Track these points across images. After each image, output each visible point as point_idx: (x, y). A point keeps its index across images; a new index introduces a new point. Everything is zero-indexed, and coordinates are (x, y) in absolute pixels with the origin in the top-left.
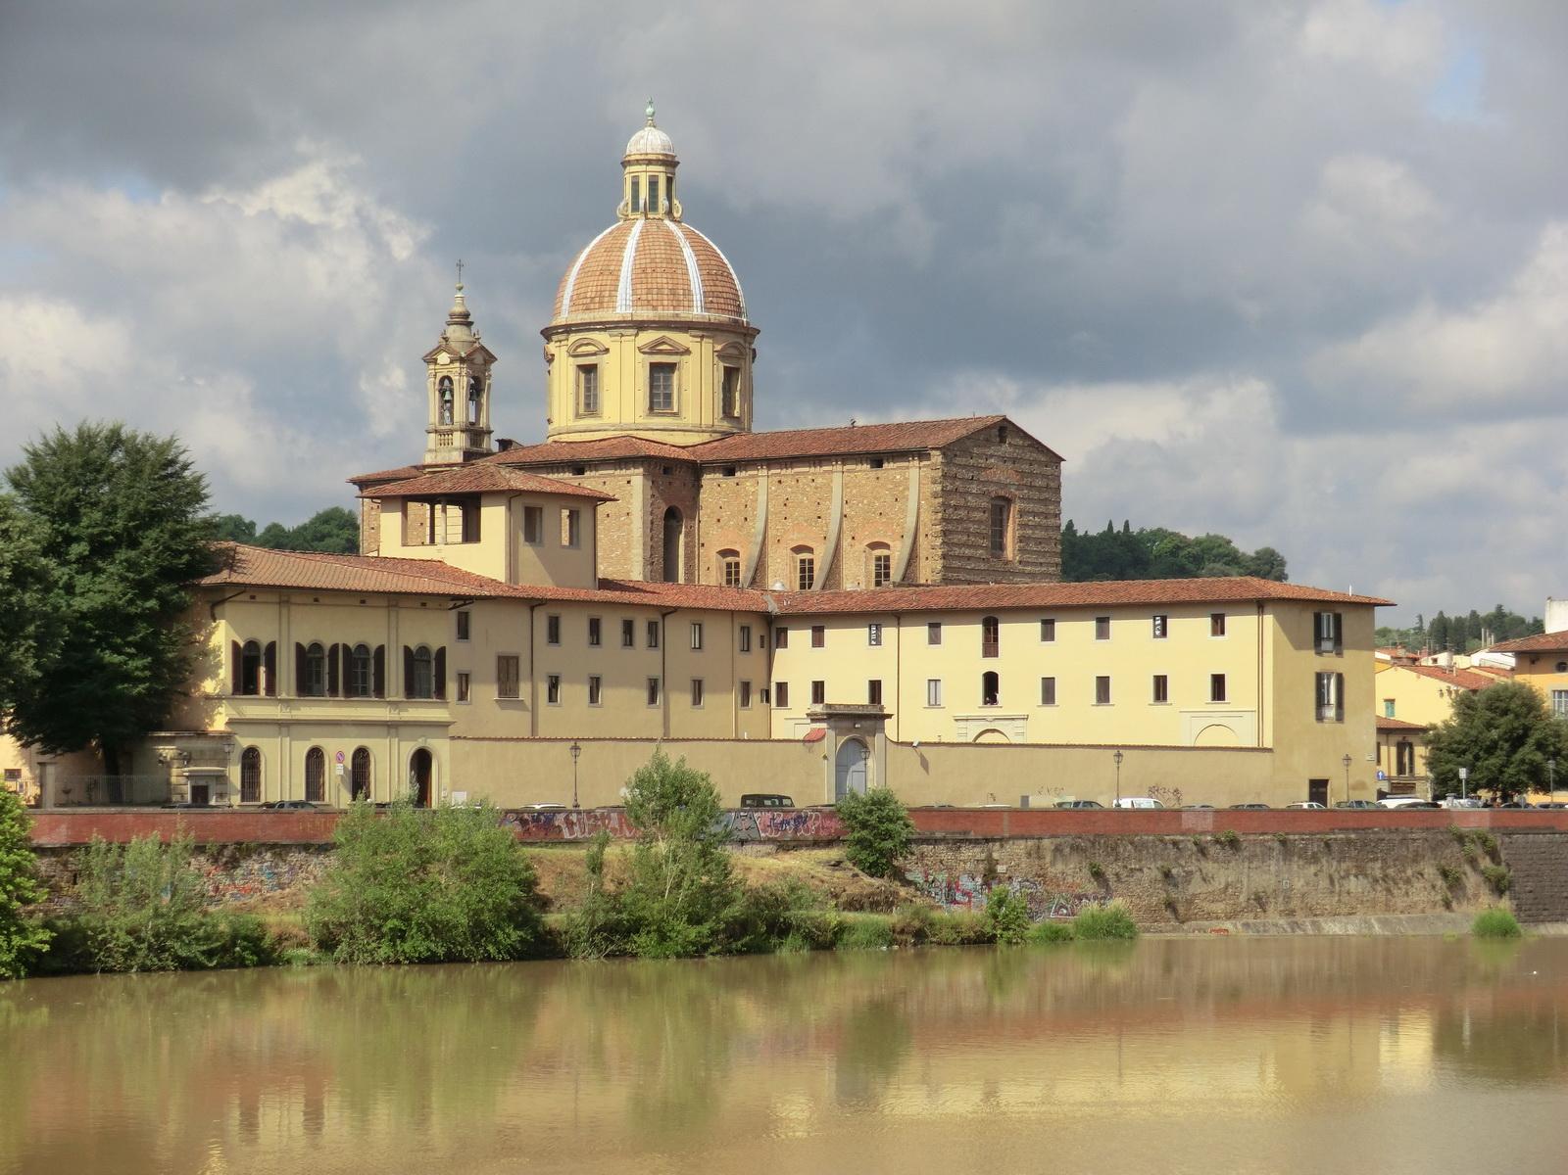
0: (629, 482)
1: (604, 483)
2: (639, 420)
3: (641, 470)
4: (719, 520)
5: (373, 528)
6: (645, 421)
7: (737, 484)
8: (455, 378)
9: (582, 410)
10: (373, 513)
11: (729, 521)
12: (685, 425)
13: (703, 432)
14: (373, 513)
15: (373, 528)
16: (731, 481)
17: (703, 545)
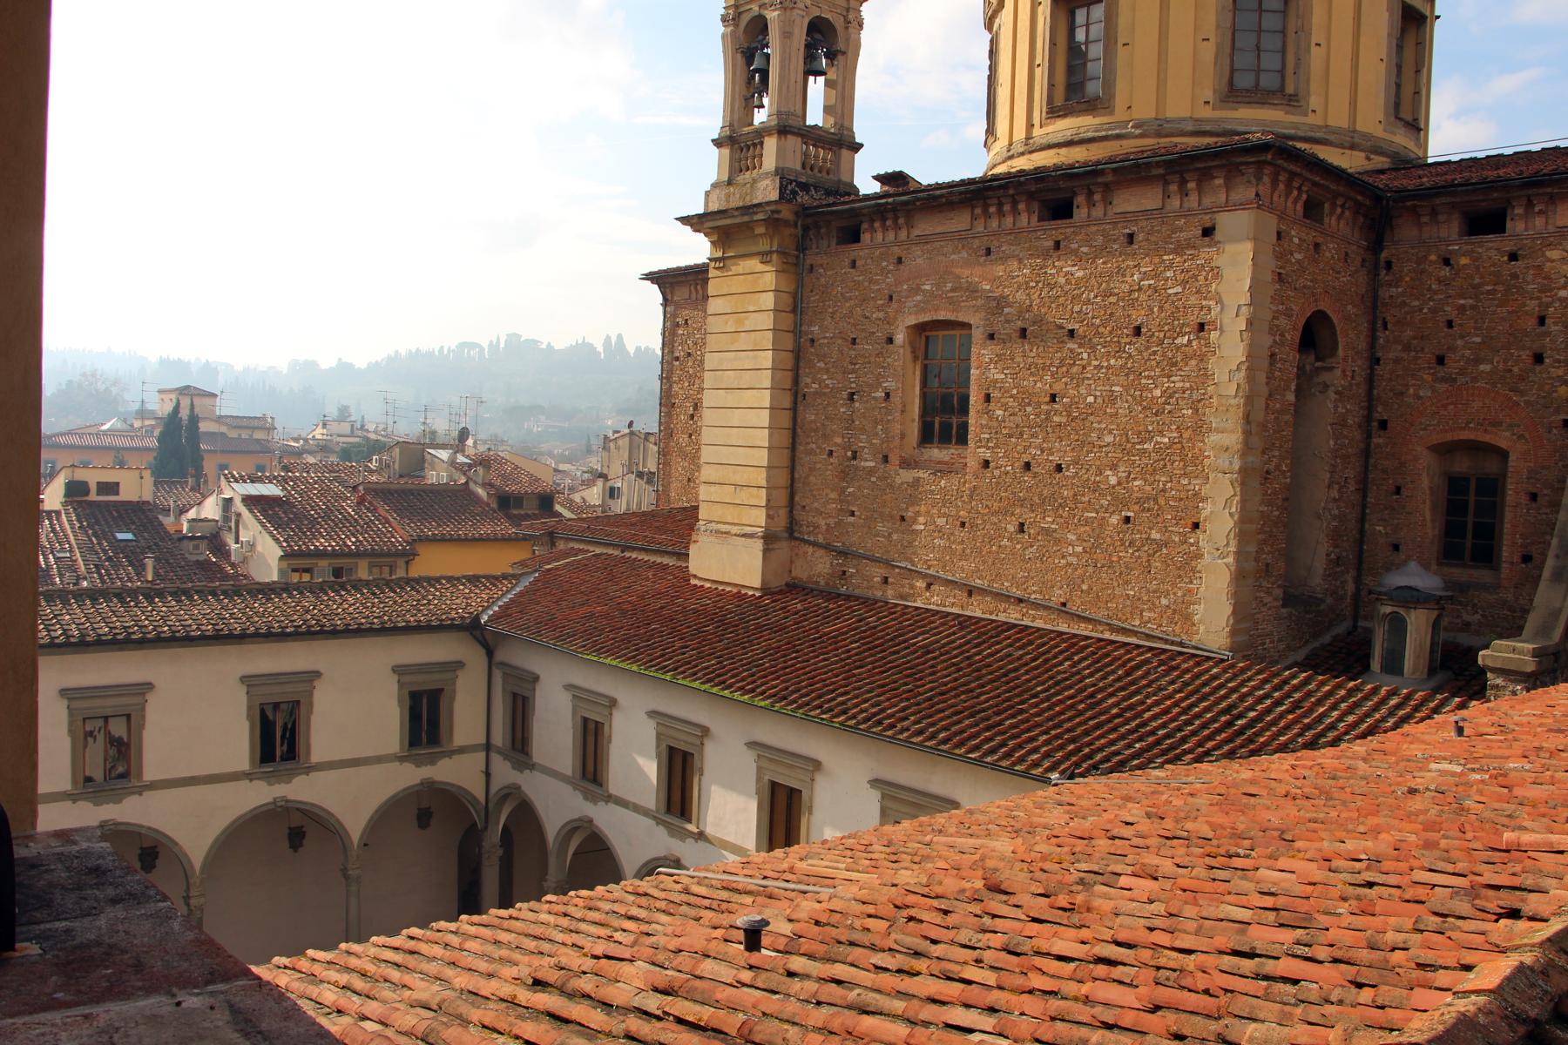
0: (1208, 232)
1: (1131, 238)
2: (1207, 113)
3: (1244, 192)
4: (1441, 360)
5: (677, 359)
6: (1218, 114)
7: (1513, 257)
8: (772, 15)
9: (1059, 101)
10: (680, 332)
11: (1478, 361)
12: (1313, 127)
13: (1352, 147)
14: (680, 332)
15: (677, 359)
16: (1491, 248)
17: (1383, 425)
